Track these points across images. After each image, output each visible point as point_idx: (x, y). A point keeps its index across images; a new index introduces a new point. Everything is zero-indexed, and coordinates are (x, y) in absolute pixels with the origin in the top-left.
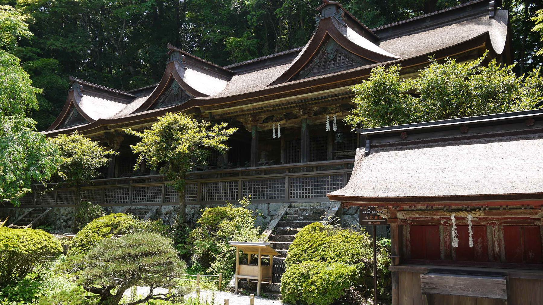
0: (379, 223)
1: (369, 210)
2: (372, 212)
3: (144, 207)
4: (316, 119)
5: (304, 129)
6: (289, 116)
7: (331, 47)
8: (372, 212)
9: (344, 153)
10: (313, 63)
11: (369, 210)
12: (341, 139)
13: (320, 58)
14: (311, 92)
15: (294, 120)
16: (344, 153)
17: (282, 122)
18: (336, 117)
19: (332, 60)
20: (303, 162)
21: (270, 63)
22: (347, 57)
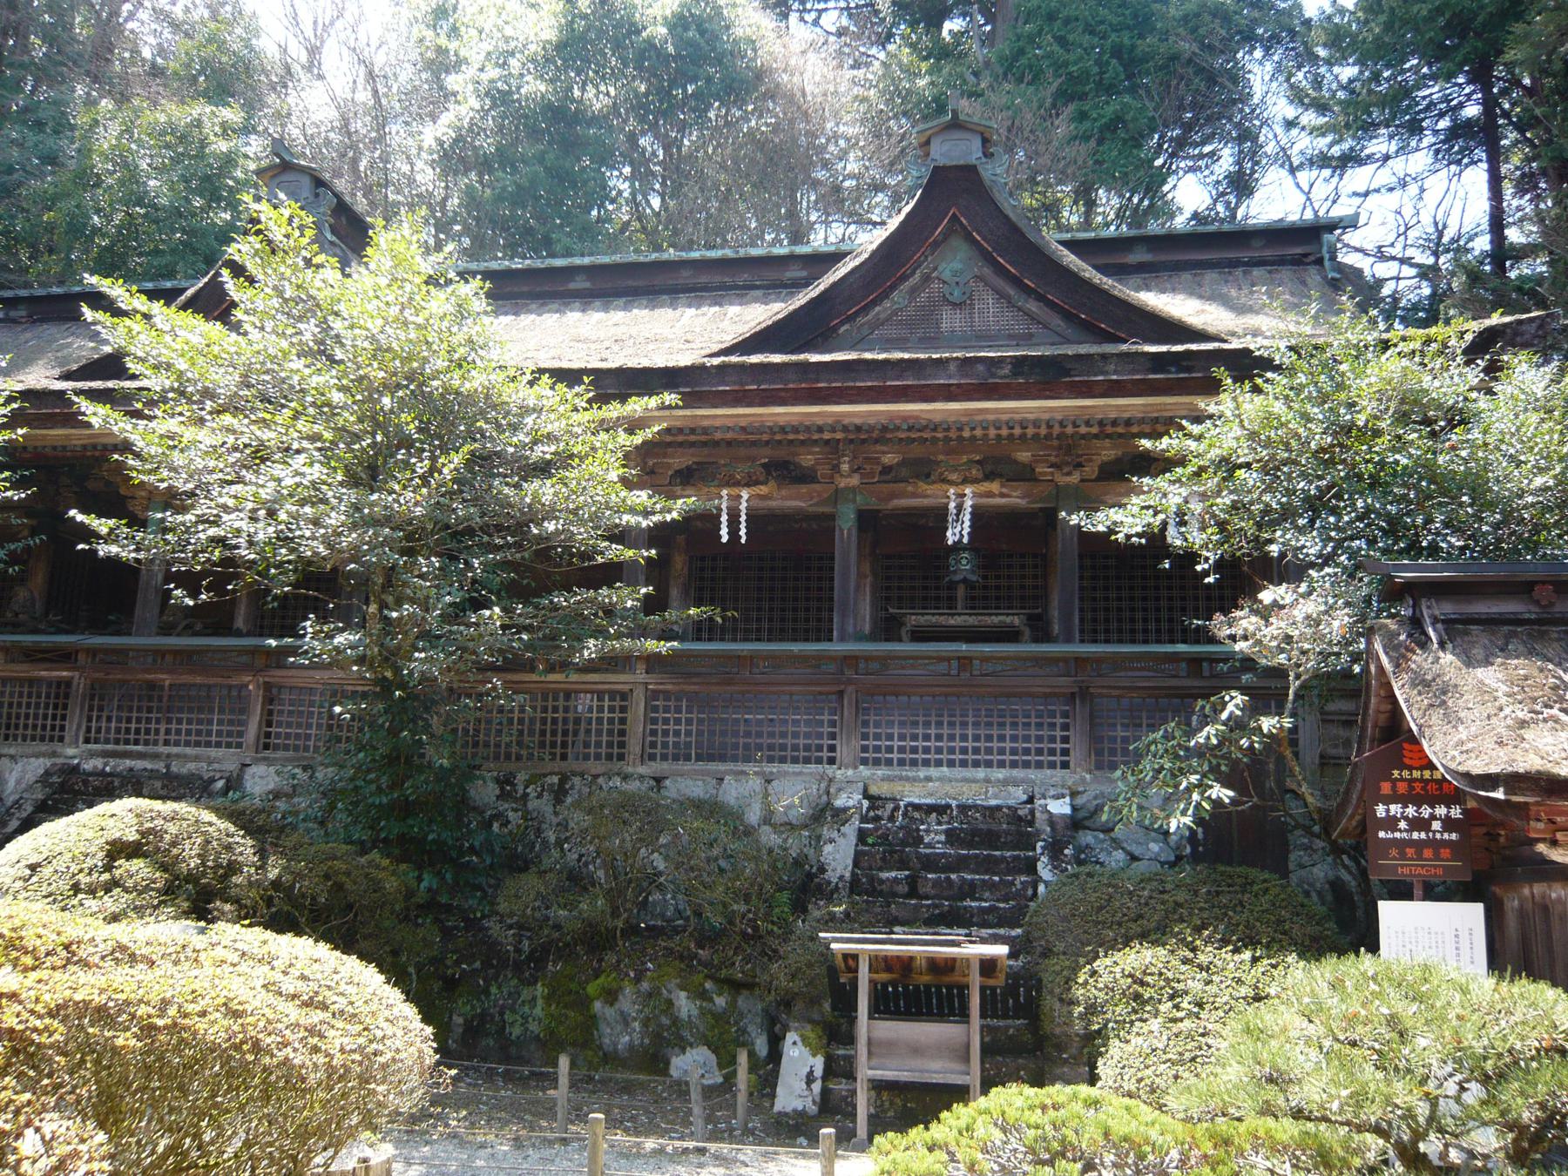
0: (1440, 872)
1: (1403, 825)
2: (1415, 835)
3: (160, 766)
4: (893, 495)
5: (847, 522)
6: (784, 471)
7: (957, 265)
8: (1415, 835)
9: (934, 619)
10: (887, 304)
11: (1403, 825)
12: (973, 572)
13: (914, 291)
14: (951, 398)
15: (804, 489)
16: (934, 619)
17: (763, 490)
18: (975, 495)
19: (954, 304)
20: (842, 639)
21: (587, 285)
22: (1010, 303)
